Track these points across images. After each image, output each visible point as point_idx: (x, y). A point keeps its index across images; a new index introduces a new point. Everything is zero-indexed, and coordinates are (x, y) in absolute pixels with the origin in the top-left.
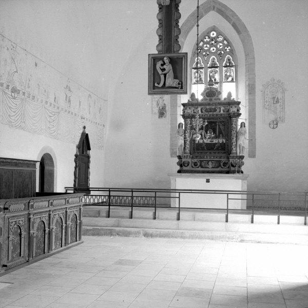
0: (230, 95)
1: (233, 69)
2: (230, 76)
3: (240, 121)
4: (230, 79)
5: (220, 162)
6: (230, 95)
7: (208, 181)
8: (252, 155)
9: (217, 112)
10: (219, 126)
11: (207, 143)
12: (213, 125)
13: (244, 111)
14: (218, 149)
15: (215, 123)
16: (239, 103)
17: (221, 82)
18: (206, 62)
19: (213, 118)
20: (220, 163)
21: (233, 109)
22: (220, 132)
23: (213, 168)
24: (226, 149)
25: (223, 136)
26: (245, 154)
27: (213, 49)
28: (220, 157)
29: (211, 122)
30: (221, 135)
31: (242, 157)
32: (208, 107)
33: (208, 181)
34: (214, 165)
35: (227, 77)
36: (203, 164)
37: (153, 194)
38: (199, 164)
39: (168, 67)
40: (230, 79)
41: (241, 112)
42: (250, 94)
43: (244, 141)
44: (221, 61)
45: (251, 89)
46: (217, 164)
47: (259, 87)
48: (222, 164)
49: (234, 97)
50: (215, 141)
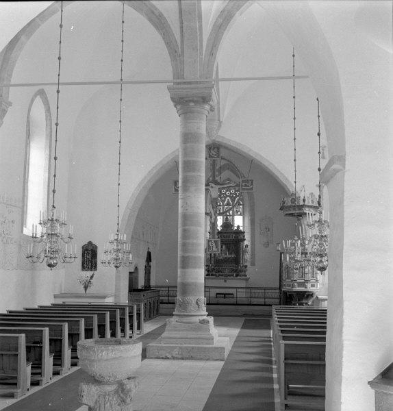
0: (238, 227)
1: (241, 206)
2: (239, 211)
3: (246, 243)
4: (239, 213)
6: (238, 227)
7: (225, 281)
8: (253, 264)
9: (231, 238)
13: (247, 237)
16: (244, 232)
17: (233, 215)
18: (223, 201)
21: (241, 236)
24: (237, 261)
26: (248, 264)
27: (228, 193)
31: (246, 266)
32: (225, 235)
33: (225, 281)
35: (237, 212)
37: (167, 289)
39: (214, 244)
40: (239, 213)
41: (245, 238)
42: (251, 225)
43: (248, 256)
44: (233, 201)
45: (252, 222)
47: (257, 220)
49: (241, 228)
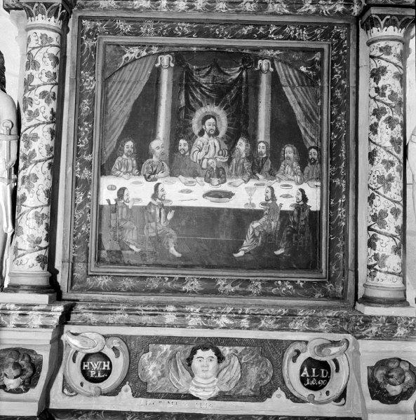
5: (272, 352)
10: (275, 78)
11: (178, 209)
12: (234, 73)
14: (264, 260)
15: (248, 59)
19: (233, 28)
20: (278, 367)
22: (285, 130)
23: (222, 396)
25: (303, 160)
28: (283, 322)
29: (220, 51)
30: (289, 151)
34: (233, 371)
36: (150, 369)
38: (119, 366)
46: (253, 372)
48: (292, 371)
50: (246, 194)
